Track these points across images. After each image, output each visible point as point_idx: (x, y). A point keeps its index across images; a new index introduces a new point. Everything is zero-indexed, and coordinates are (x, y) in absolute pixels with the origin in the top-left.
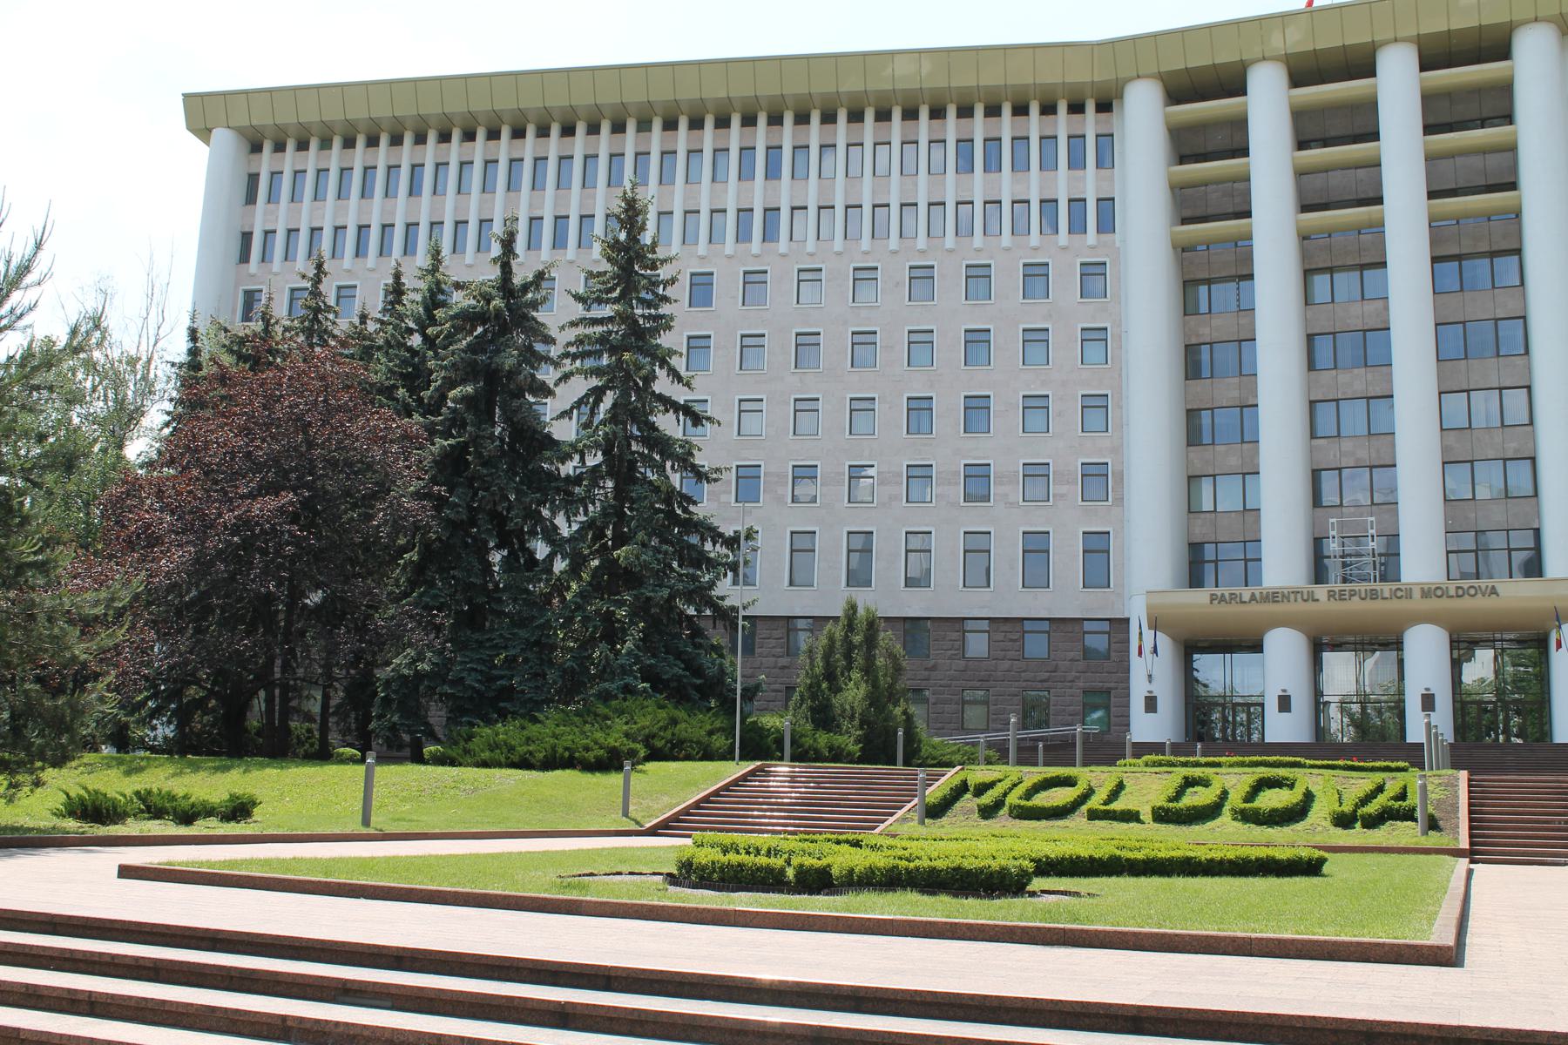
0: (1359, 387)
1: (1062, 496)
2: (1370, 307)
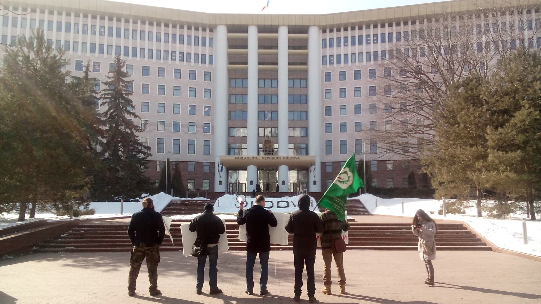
0: (269, 109)
1: (199, 131)
2: (273, 89)
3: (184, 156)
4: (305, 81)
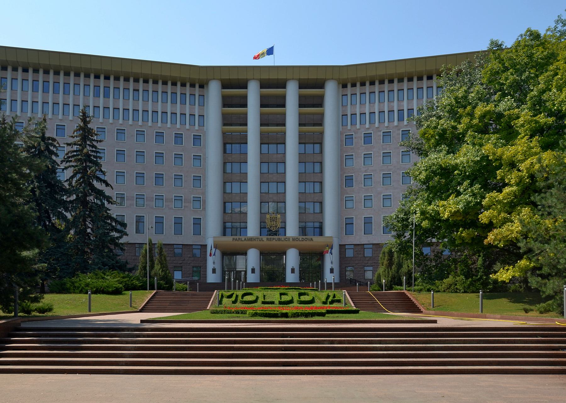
3: (168, 237)
4: (319, 145)
